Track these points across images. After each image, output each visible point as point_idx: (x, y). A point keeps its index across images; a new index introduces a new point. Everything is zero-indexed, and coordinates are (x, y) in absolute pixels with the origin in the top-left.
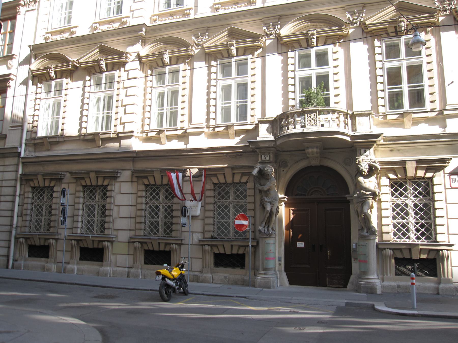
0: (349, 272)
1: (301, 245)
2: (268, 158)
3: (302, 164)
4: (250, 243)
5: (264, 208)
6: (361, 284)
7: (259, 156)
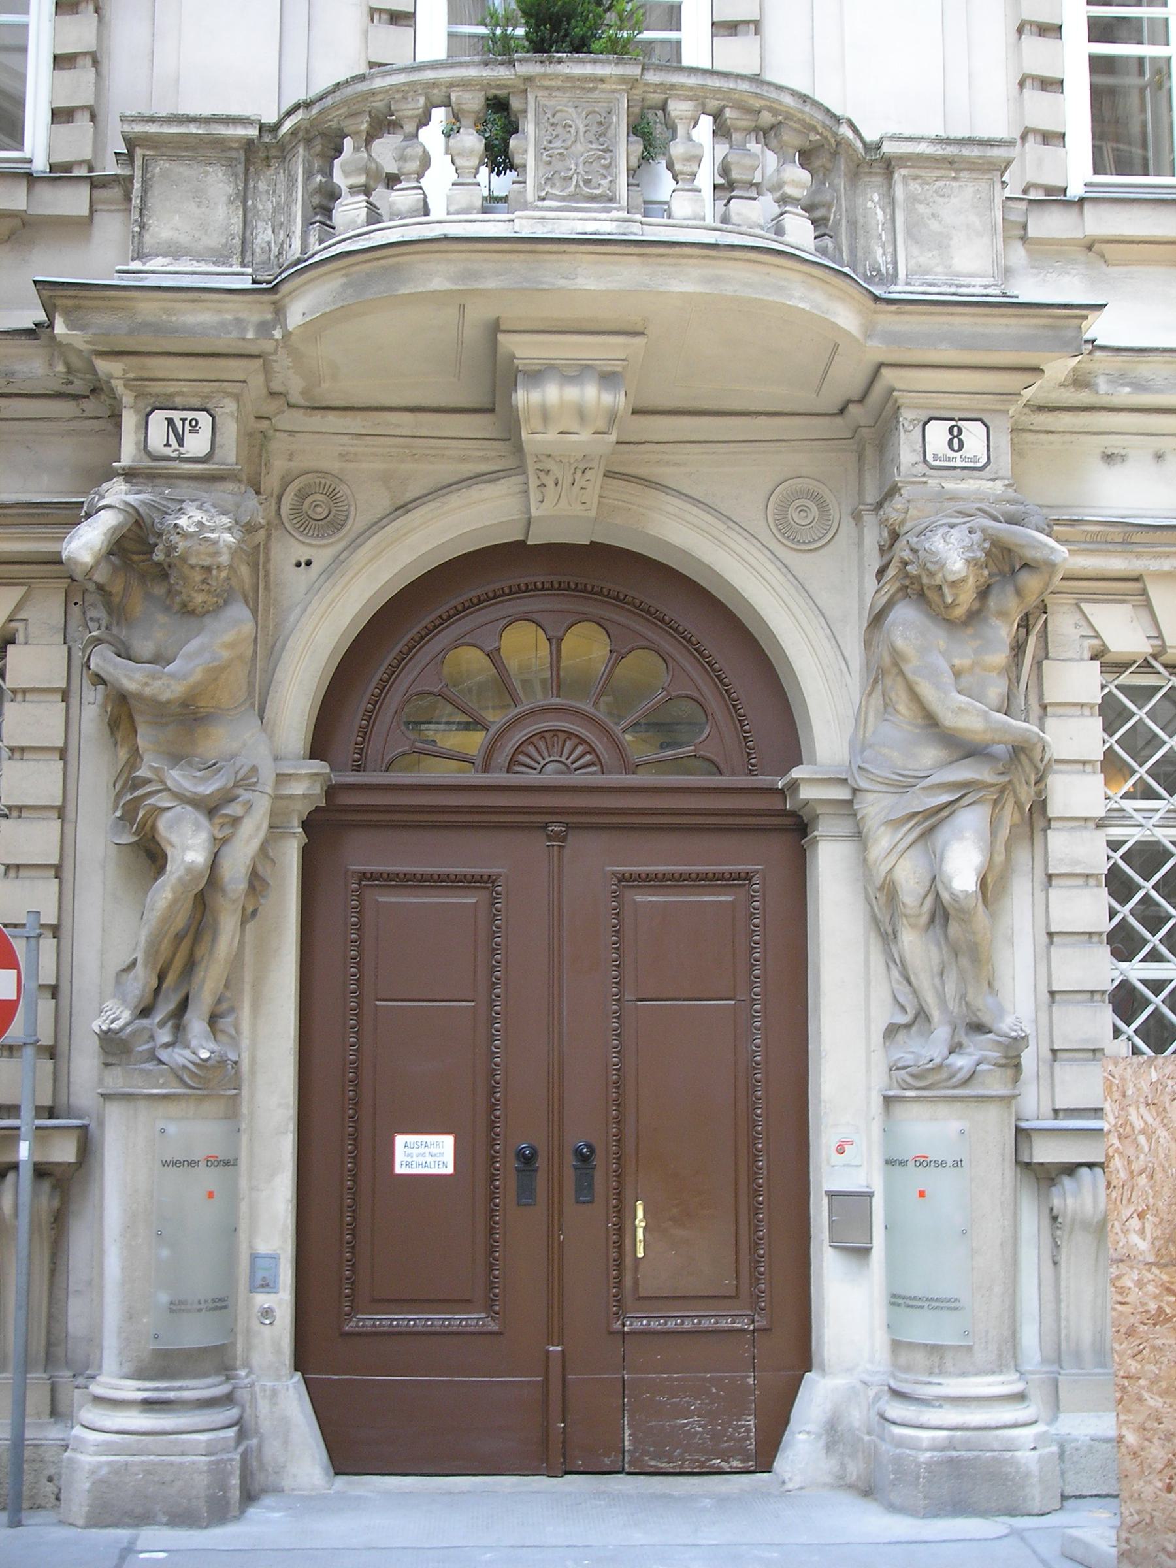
0: (794, 1348)
1: (425, 1154)
2: (197, 444)
3: (478, 516)
4: (24, 1151)
5: (150, 855)
6: (915, 1445)
7: (129, 420)
